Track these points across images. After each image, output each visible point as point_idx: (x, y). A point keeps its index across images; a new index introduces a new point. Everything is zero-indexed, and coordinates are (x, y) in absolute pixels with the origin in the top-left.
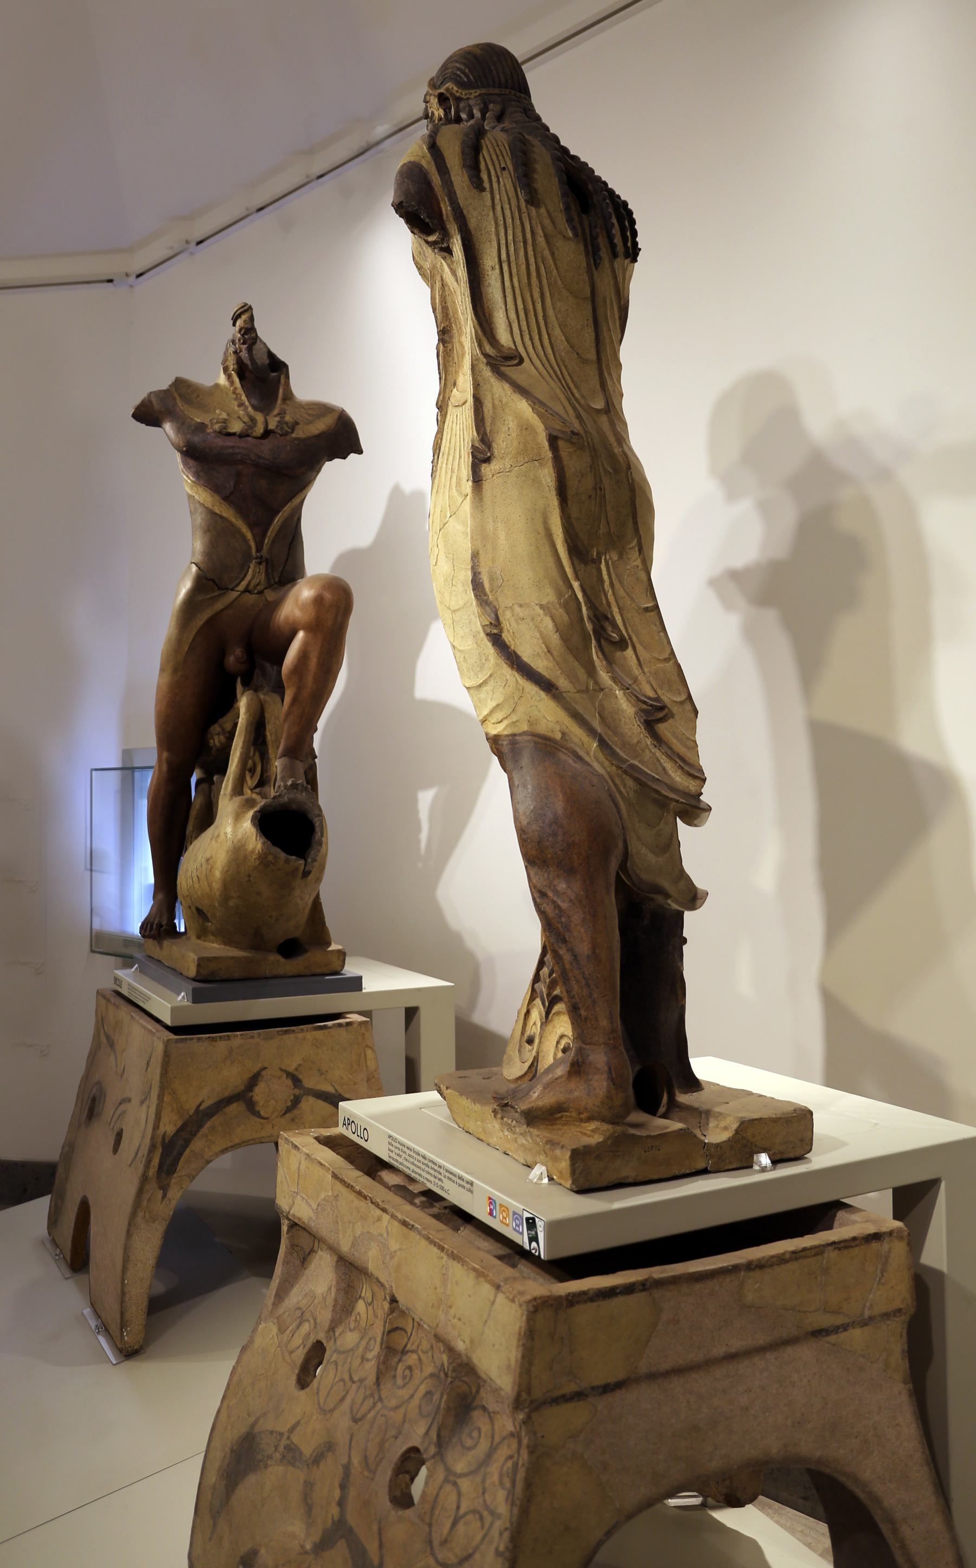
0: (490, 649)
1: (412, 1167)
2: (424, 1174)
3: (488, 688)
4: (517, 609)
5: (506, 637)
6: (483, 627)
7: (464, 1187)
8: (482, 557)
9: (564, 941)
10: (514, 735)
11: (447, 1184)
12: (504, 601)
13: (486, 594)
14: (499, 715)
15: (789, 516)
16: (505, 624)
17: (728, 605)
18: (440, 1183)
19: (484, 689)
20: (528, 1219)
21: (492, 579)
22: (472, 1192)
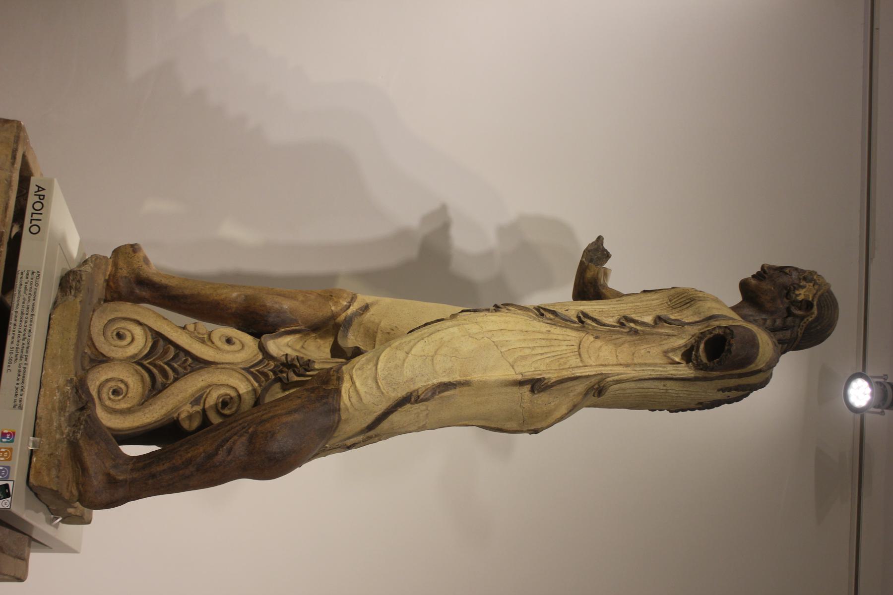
0: (401, 393)
1: (19, 310)
2: (17, 327)
3: (375, 390)
4: (425, 413)
5: (408, 406)
6: (417, 390)
7: (16, 396)
8: (465, 389)
9: (198, 470)
10: (339, 410)
11: (15, 367)
12: (431, 404)
13: (439, 393)
14: (354, 400)
15: (478, 274)
16: (416, 406)
17: (426, 219)
18: (13, 359)
19: (374, 386)
20: (7, 486)
21: (449, 397)
22: (14, 407)
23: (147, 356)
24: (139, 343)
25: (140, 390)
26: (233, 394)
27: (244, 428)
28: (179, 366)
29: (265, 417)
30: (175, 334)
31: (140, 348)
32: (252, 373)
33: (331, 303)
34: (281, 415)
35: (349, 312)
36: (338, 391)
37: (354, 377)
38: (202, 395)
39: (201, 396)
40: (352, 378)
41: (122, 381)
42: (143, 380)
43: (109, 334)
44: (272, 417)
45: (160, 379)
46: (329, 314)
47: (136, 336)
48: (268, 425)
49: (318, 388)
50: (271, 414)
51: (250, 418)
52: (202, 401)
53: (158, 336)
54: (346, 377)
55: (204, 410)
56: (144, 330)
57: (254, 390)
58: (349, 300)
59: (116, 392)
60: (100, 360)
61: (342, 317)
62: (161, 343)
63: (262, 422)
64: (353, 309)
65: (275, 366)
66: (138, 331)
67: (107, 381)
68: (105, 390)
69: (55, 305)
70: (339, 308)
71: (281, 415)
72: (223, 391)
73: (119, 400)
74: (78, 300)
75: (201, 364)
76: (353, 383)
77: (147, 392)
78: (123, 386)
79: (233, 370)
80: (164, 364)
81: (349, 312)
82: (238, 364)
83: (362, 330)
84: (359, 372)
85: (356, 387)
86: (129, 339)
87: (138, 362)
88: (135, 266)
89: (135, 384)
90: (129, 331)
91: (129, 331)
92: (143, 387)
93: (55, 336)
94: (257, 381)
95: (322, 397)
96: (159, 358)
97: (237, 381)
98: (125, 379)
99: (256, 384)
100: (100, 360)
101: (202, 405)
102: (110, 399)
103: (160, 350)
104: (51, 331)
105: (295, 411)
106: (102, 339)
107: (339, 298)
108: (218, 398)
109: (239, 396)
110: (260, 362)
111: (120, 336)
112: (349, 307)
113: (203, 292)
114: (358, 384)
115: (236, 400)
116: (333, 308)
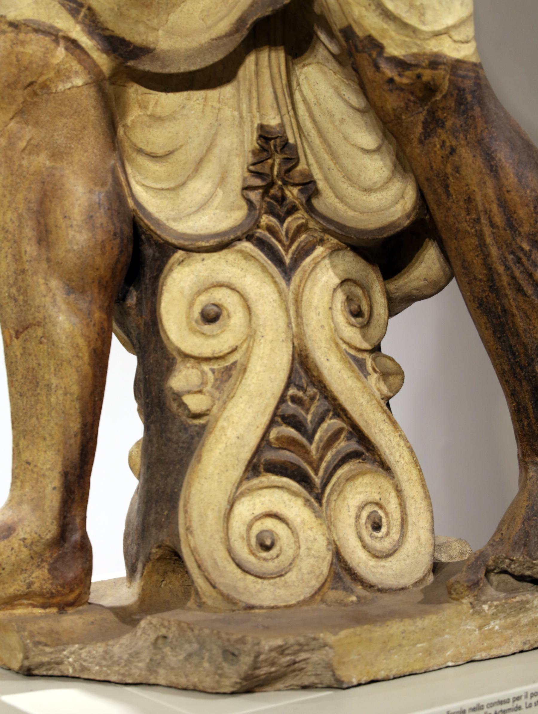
23: (303, 479)
24: (279, 497)
25: (367, 479)
26: (340, 297)
27: (519, 261)
28: (307, 411)
29: (499, 220)
30: (231, 433)
31: (286, 496)
32: (297, 260)
33: (61, 87)
34: (500, 188)
35: (86, 41)
36: (457, 65)
37: (438, 27)
38: (354, 358)
39: (354, 358)
40: (437, 34)
41: (358, 517)
42: (350, 478)
43: (271, 566)
44: (503, 204)
45: (343, 445)
46: (92, 91)
47: (259, 510)
48: (522, 213)
49: (432, 113)
50: (495, 208)
51: (494, 251)
52: (360, 356)
53: (260, 464)
54: (433, 46)
55: (371, 351)
56: (243, 494)
57: (335, 251)
58: (47, 41)
59: (377, 527)
60: (341, 571)
61: (103, 61)
62: (269, 455)
63: (512, 224)
64: (77, 32)
65: (271, 212)
66: (245, 510)
67: (364, 546)
68: (378, 545)
69: (339, 685)
70: (76, 66)
71: (500, 188)
72: (341, 318)
73: (387, 514)
74: (331, 638)
75: (302, 367)
76: (446, 31)
77: (368, 466)
78: (364, 514)
79: (298, 301)
80: (312, 441)
81: (86, 41)
82: (280, 293)
83: (134, 13)
84: (429, 16)
85: (455, 27)
86: (269, 524)
87: (315, 492)
88: (25, 553)
89: (357, 492)
90: (250, 527)
91: (250, 527)
92: (362, 473)
93: (395, 663)
94: (313, 249)
95: (461, 101)
96: (305, 452)
97: (317, 290)
98: (353, 512)
99: (319, 250)
100: (341, 571)
101: (366, 356)
102: (388, 534)
103: (287, 456)
104: (382, 674)
105: (489, 157)
106: (291, 576)
107: (46, 65)
108: (352, 325)
109: (344, 282)
110: (261, 244)
111: (265, 545)
112: (73, 45)
113: (75, 389)
114: (450, 21)
115: (346, 287)
116: (79, 81)
